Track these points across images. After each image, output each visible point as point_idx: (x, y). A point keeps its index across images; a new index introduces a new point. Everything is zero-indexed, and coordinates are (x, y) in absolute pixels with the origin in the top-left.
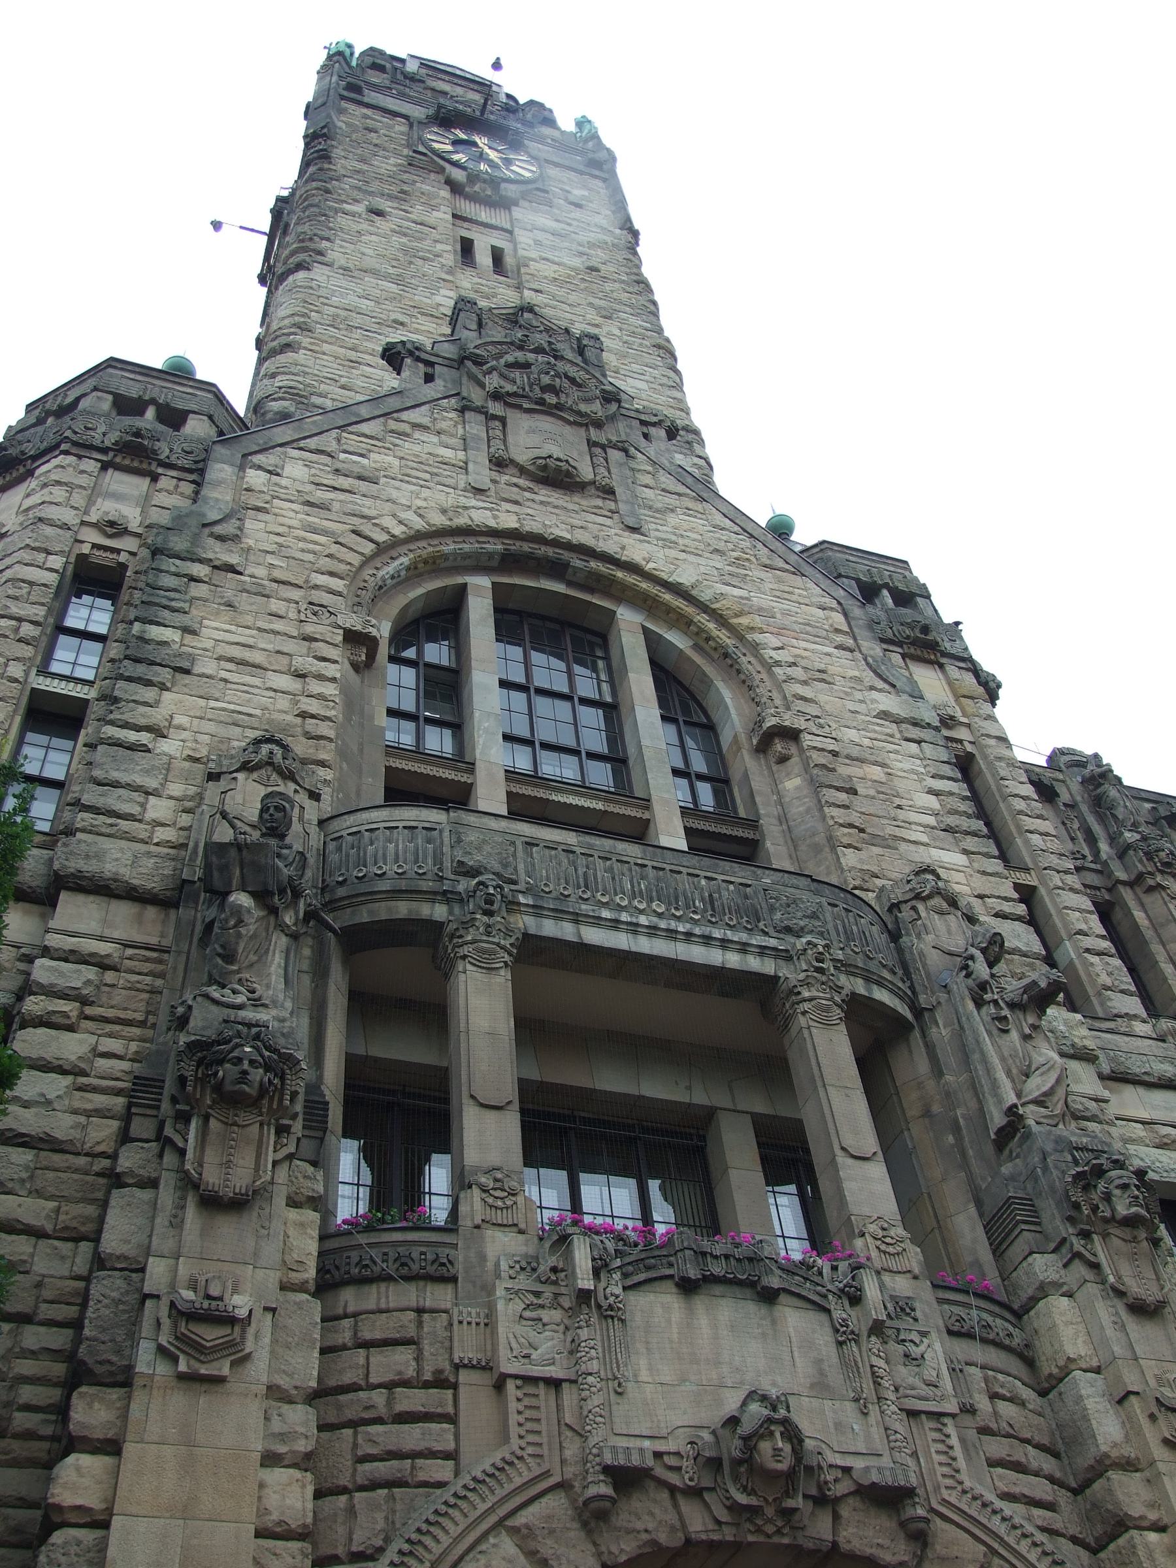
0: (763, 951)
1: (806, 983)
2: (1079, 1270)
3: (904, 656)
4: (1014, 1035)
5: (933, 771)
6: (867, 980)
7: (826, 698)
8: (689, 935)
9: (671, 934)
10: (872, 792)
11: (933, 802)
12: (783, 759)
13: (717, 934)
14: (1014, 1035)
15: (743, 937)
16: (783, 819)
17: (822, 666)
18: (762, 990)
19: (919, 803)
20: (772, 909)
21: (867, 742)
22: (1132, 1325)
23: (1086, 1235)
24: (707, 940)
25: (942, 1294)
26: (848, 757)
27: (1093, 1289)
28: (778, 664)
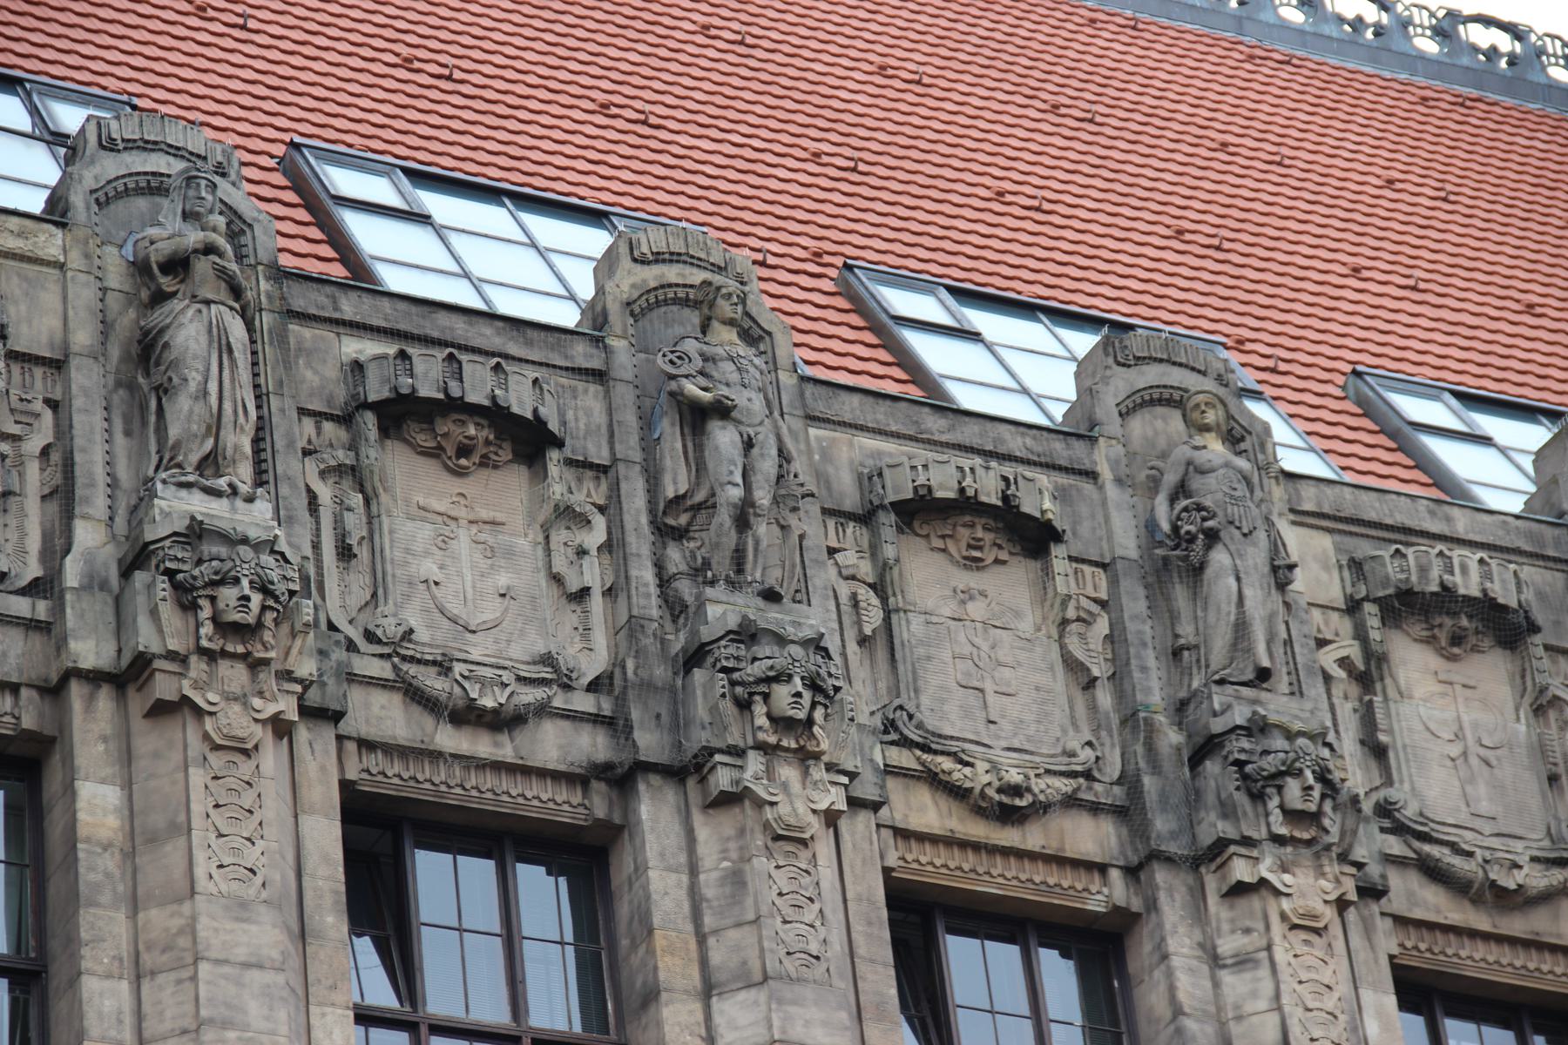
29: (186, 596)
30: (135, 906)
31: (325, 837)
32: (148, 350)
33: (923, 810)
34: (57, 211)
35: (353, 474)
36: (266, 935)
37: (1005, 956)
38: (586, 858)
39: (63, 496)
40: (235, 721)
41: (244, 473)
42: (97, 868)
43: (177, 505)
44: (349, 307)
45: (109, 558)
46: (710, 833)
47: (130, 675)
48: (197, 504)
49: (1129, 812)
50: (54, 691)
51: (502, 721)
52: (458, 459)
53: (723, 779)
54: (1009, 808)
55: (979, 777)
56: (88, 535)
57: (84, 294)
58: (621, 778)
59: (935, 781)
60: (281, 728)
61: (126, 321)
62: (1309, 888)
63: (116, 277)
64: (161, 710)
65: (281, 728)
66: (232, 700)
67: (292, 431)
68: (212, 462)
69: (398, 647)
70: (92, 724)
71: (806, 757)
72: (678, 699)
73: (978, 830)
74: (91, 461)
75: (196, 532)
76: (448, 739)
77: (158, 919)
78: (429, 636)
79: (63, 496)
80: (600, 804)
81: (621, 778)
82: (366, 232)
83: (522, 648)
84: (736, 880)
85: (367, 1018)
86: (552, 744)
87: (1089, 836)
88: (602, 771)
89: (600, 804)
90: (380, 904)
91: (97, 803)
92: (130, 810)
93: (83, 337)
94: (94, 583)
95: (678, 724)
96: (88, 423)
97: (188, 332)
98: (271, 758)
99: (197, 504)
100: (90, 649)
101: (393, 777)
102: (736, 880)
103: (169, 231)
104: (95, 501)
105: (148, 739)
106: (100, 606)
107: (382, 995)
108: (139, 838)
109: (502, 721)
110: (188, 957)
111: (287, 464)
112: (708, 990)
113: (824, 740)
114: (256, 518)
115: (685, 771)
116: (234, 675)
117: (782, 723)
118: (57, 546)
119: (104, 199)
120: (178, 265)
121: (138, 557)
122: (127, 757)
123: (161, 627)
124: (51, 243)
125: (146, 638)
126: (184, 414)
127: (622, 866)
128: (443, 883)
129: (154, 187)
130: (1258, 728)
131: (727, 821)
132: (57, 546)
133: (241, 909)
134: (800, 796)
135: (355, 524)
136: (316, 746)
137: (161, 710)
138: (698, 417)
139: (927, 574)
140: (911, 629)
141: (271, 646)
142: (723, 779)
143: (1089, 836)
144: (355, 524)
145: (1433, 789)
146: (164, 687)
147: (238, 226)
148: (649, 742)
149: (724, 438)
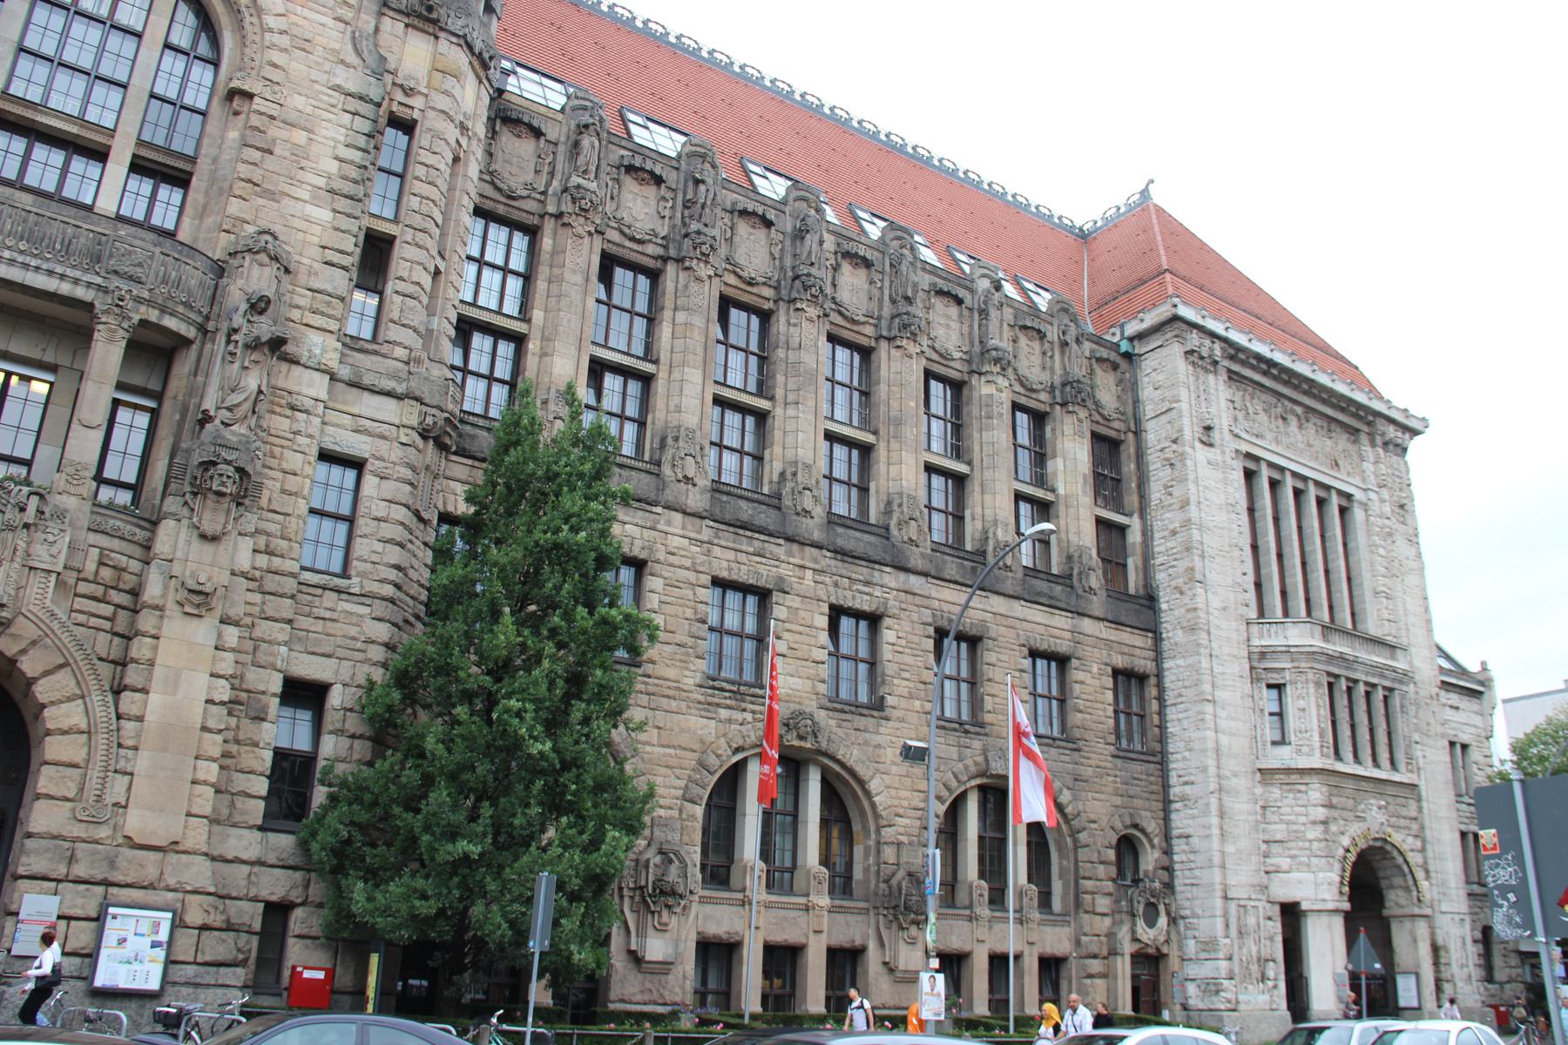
0: (89, 285)
1: (106, 312)
2: (186, 512)
3: (407, 26)
4: (237, 365)
5: (349, 140)
6: (163, 311)
7: (297, 66)
8: (37, 268)
9: (26, 266)
10: (287, 154)
11: (333, 167)
12: (236, 113)
13: (59, 269)
14: (237, 365)
15: (78, 274)
16: (215, 160)
17: (309, 36)
18: (91, 306)
19: (321, 166)
20: (111, 256)
21: (309, 110)
22: (196, 544)
23: (195, 494)
24: (50, 273)
25: (96, 509)
26: (284, 122)
27: (185, 522)
28: (271, 30)
29: (574, 200)
30: (551, 266)
31: (596, 260)
32: (576, 144)
33: (732, 280)
34: (562, 111)
35: (617, 180)
36: (579, 279)
37: (744, 315)
38: (654, 276)
39: (552, 174)
40: (580, 230)
41: (592, 176)
42: (544, 257)
43: (576, 180)
44: (623, 143)
45: (559, 189)
46: (682, 275)
47: (558, 216)
48: (580, 180)
49: (777, 289)
50: (542, 216)
51: (640, 242)
52: (642, 181)
53: (687, 264)
54: (751, 282)
55: (745, 274)
56: (555, 183)
57: (565, 129)
58: (665, 259)
59: (735, 273)
60: (590, 234)
61: (573, 137)
62: (812, 312)
63: (573, 127)
64: (564, 225)
65: (590, 234)
66: (580, 226)
67: (605, 168)
68: (585, 172)
69: (620, 221)
70: (549, 225)
71: (707, 262)
72: (681, 244)
73: (743, 286)
74: (559, 167)
75: (578, 187)
76: (628, 243)
77: (556, 271)
78: (627, 220)
79: (552, 174)
80: (659, 264)
81: (665, 259)
82: (633, 129)
83: (648, 226)
84: (686, 286)
85: (598, 301)
86: (651, 249)
87: (767, 292)
88: (660, 257)
89: (659, 264)
90: (606, 277)
91: (547, 243)
92: (554, 246)
93: (563, 139)
94: (555, 194)
95: (680, 250)
96: (560, 158)
97: (586, 142)
98: (587, 240)
99: (580, 180)
100: (551, 209)
101: (613, 249)
102: (686, 286)
103: (586, 119)
104: (558, 176)
105: (561, 231)
106: (555, 200)
107: (603, 297)
108: (555, 252)
109: (640, 242)
110: (561, 280)
111: (603, 175)
112: (675, 309)
113: (711, 259)
114: (593, 186)
115: (679, 260)
116: (582, 220)
117: (703, 254)
118: (548, 184)
119: (574, 109)
120: (586, 126)
121: (565, 190)
122: (555, 234)
123: (568, 207)
124: (560, 117)
125: (564, 208)
126: (581, 160)
127: (661, 279)
128: (621, 276)
129: (585, 108)
130: (809, 275)
131: (686, 273)
132: (548, 184)
133: (574, 272)
134: (704, 271)
135: (615, 192)
136: (597, 240)
137: (564, 225)
138: (698, 182)
139: (743, 227)
140: (736, 239)
141: (591, 215)
142: (687, 264)
143: (767, 292)
144: (615, 192)
145: (844, 296)
146: (566, 220)
147: (601, 120)
148: (672, 253)
149: (702, 188)
